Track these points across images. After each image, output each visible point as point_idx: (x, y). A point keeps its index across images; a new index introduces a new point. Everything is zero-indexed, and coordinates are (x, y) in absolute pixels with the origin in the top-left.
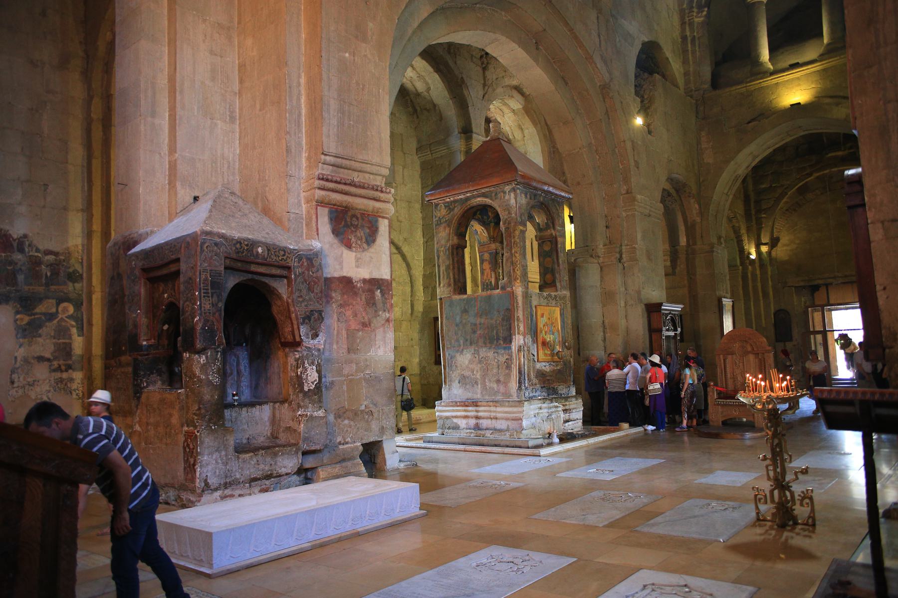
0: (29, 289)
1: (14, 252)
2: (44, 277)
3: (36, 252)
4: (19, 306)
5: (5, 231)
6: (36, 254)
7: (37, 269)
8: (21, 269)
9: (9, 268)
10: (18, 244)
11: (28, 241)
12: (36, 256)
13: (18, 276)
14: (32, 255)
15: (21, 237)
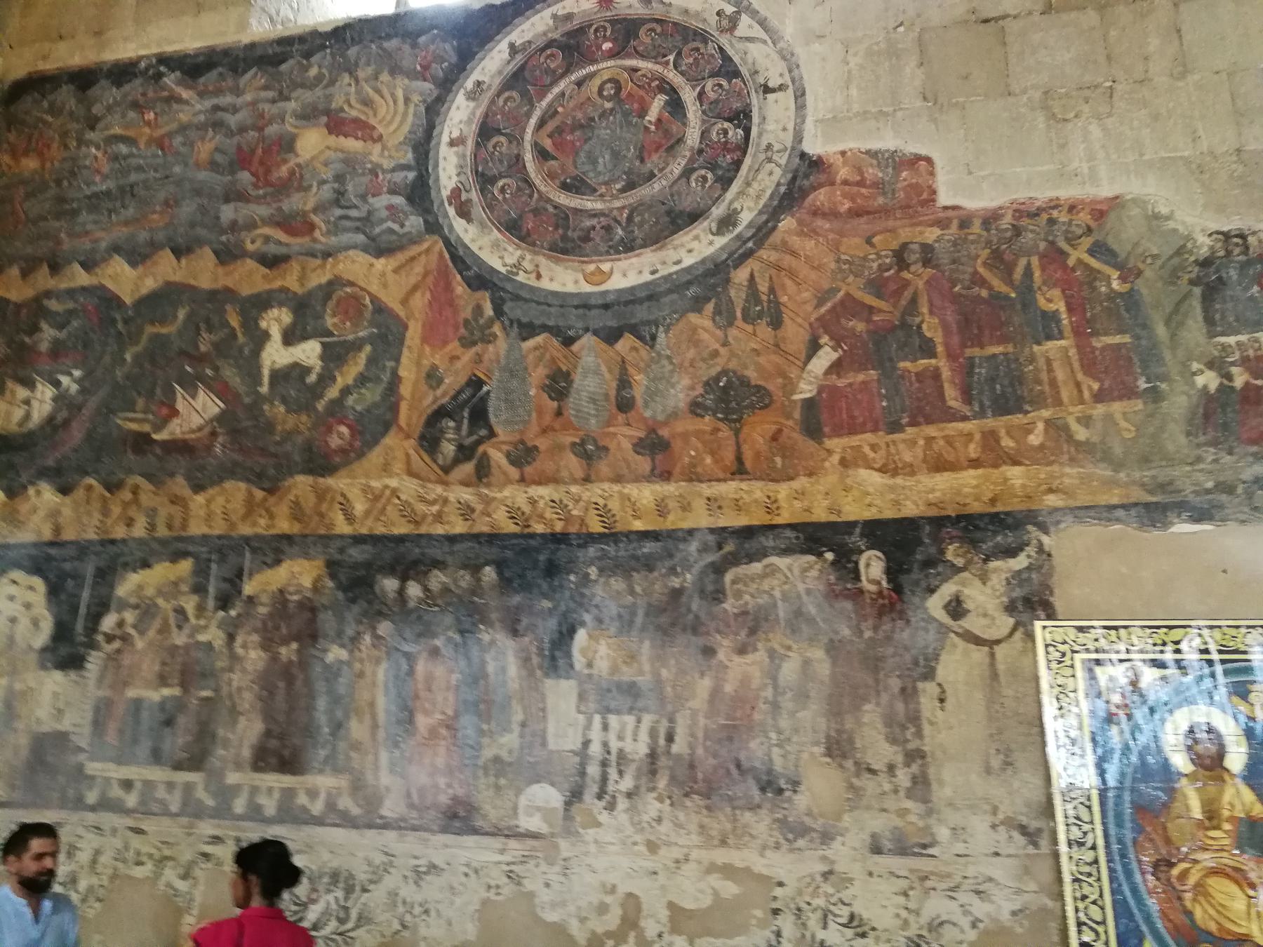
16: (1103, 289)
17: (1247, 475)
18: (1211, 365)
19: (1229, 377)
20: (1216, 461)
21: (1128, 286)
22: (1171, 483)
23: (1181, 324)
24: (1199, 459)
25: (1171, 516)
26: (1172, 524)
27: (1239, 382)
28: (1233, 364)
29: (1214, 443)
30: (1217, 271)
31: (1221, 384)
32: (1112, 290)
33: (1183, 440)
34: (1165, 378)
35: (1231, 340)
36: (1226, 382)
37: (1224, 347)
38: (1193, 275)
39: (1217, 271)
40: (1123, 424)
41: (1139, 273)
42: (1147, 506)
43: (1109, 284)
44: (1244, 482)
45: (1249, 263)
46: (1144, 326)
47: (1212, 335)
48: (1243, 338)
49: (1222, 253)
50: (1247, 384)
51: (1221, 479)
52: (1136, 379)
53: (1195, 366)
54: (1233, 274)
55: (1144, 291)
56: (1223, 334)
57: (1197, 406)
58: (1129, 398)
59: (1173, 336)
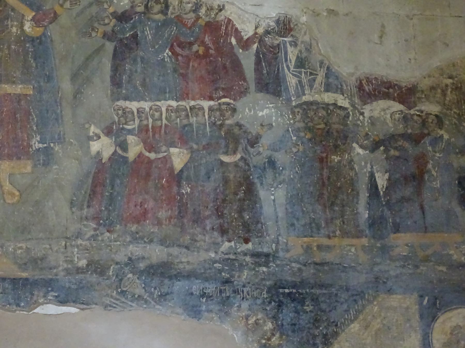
0: (308, 249)
1: (244, 92)
2: (364, 196)
3: (328, 88)
4: (269, 325)
5: (210, 9)
6: (328, 98)
7: (336, 158)
8: (272, 163)
9: (226, 159)
10: (258, 63)
11: (294, 44)
12: (326, 107)
13: (262, 193)
14: (312, 103)
15: (267, 32)
16: (14, 30)
17: (121, 257)
18: (108, 132)
19: (123, 146)
20: (94, 237)
21: (40, 30)
22: (43, 259)
23: (88, 80)
24: (79, 235)
25: (38, 294)
26: (37, 304)
27: (132, 154)
28: (130, 132)
29: (96, 218)
30: (133, 27)
31: (115, 151)
32: (23, 30)
33: (65, 210)
34: (61, 140)
35: (134, 106)
36: (120, 152)
37: (125, 112)
38: (109, 29)
39: (133, 27)
40: (7, 186)
41: (56, 16)
42: (14, 281)
43: (22, 26)
44: (117, 263)
45: (166, 24)
46: (49, 78)
47: (115, 97)
48: (146, 105)
49: (140, 9)
50: (140, 155)
51: (96, 258)
52: (30, 137)
53: (93, 129)
54: (149, 34)
55: (56, 38)
56: (126, 98)
57: (87, 175)
58: (19, 158)
59: (77, 94)
